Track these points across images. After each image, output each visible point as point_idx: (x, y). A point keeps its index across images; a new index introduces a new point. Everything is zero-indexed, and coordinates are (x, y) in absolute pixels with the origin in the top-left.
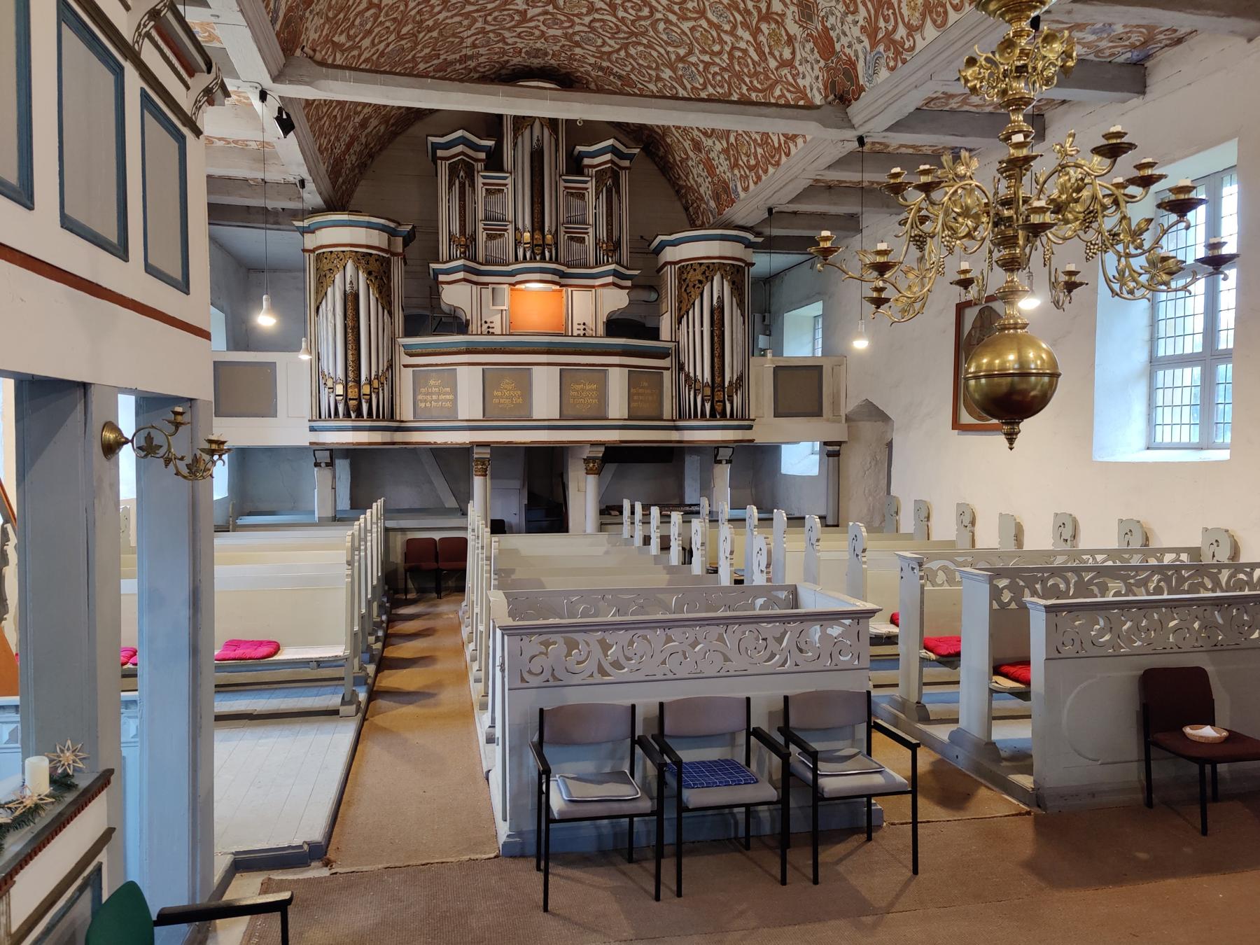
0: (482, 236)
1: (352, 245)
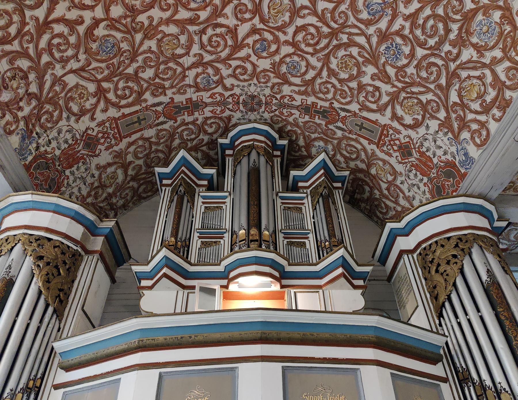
0: (196, 243)
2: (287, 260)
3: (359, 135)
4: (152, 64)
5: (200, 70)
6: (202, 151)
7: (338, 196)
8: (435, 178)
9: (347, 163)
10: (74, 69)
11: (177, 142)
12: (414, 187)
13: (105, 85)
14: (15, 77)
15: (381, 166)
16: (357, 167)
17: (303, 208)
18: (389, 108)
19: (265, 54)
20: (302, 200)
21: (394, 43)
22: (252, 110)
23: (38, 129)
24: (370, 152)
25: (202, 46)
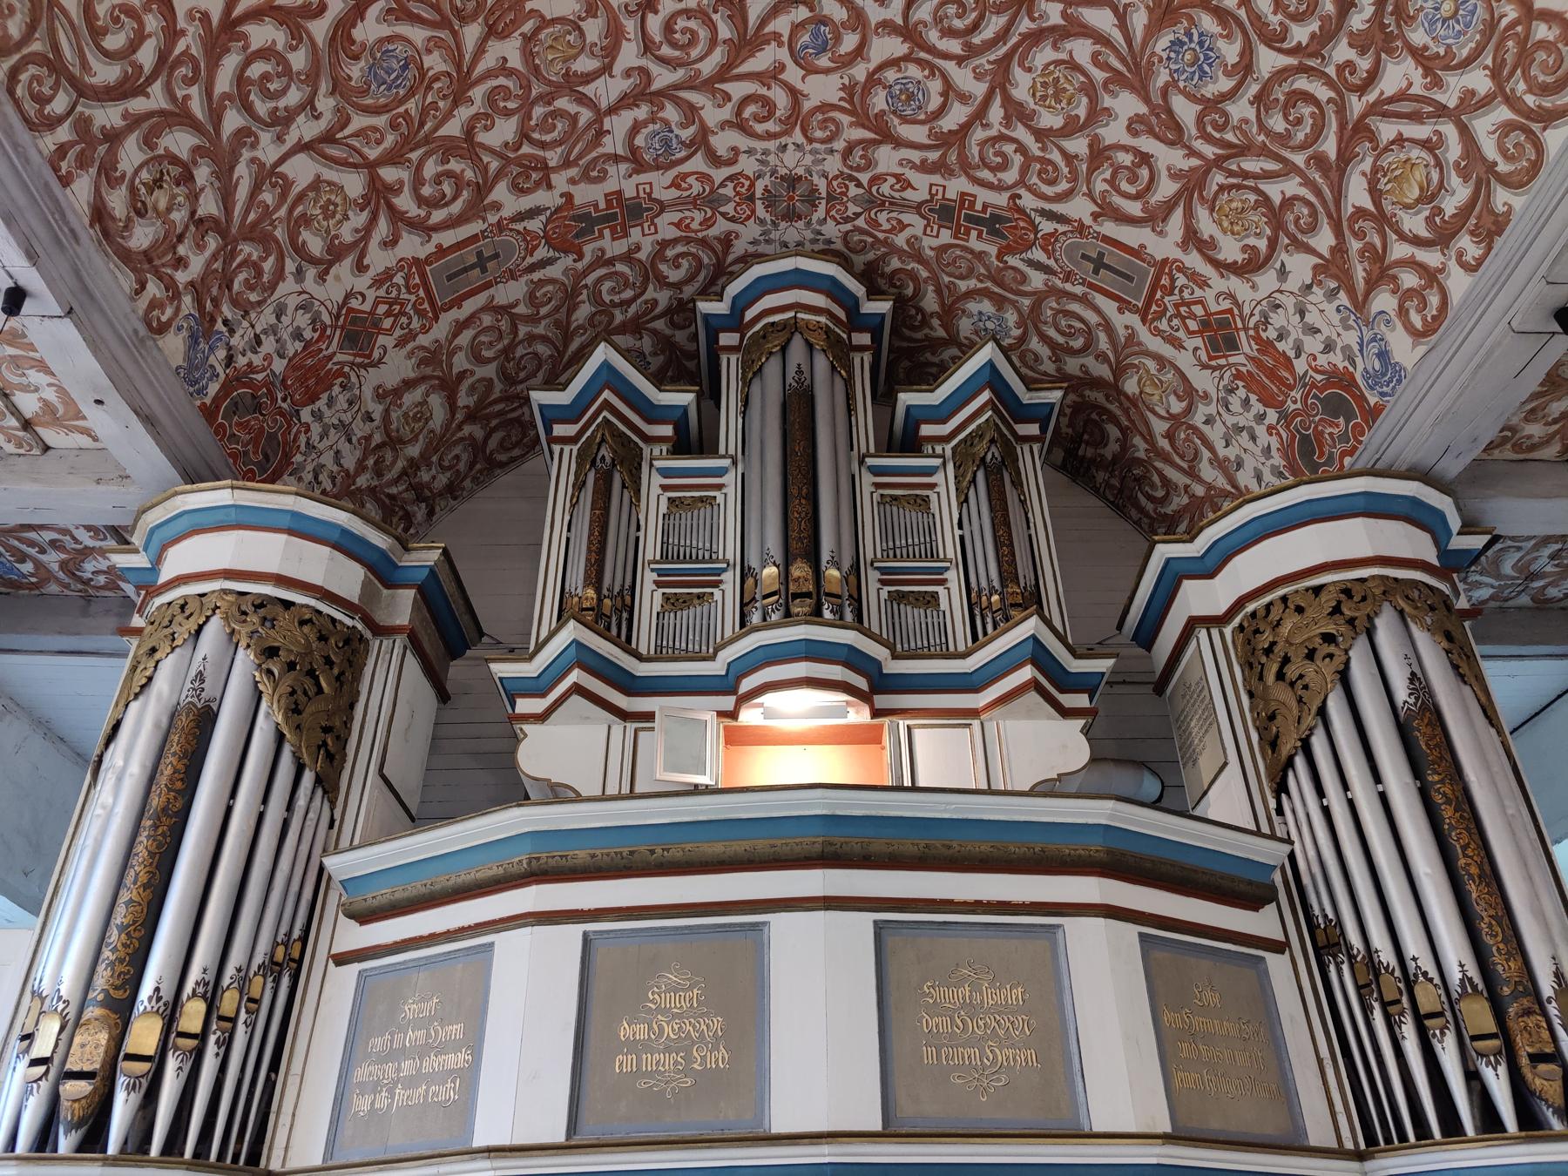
0: (649, 599)
1: (229, 574)
2: (890, 646)
3: (1091, 286)
4: (511, 105)
5: (642, 112)
6: (654, 332)
7: (1030, 462)
8: (1296, 413)
9: (1057, 360)
10: (307, 139)
11: (584, 311)
12: (1240, 436)
13: (389, 174)
14: (161, 179)
15: (1153, 371)
16: (1087, 372)
17: (934, 497)
18: (1178, 215)
19: (824, 61)
20: (931, 475)
21: (1194, 31)
22: (791, 216)
23: (227, 311)
24: (1122, 333)
25: (648, 47)
